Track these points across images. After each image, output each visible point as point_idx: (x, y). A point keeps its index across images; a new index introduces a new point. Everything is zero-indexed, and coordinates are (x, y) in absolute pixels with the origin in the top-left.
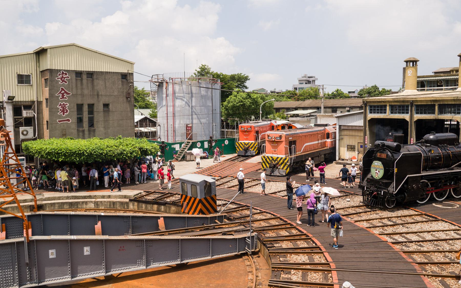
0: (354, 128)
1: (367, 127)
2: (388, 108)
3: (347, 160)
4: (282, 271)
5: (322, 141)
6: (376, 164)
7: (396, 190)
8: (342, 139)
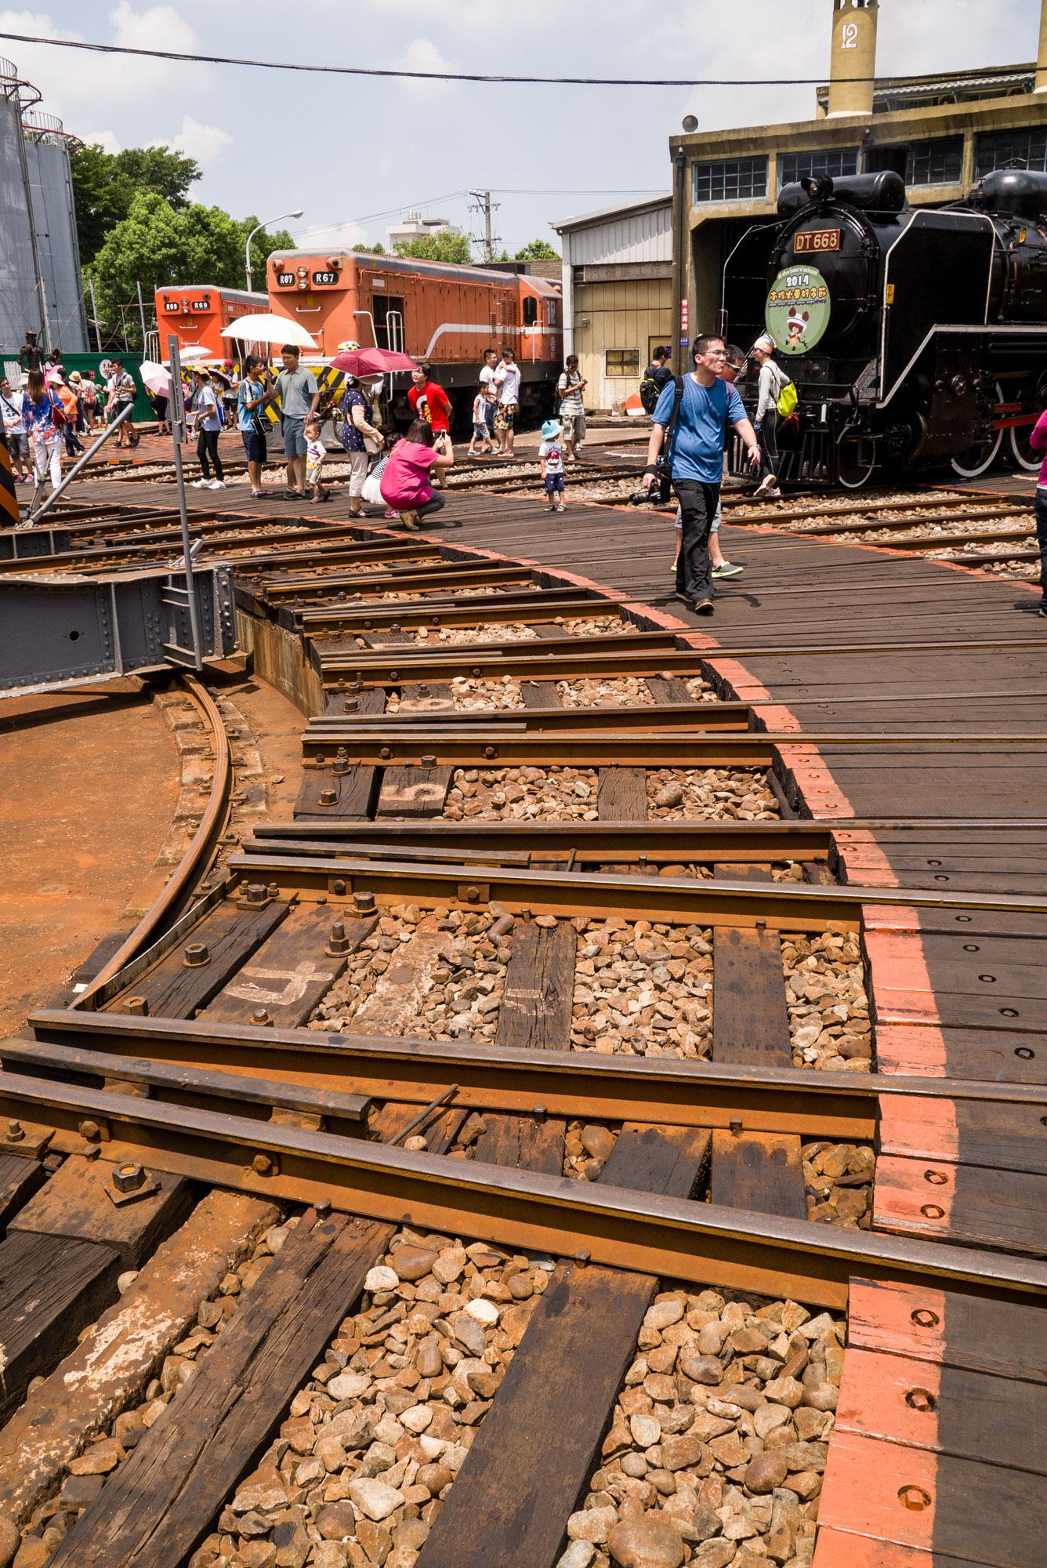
0: (634, 274)
1: (689, 259)
2: (772, 167)
3: (609, 413)
4: (389, 691)
5: (508, 330)
6: (792, 282)
7: (885, 394)
8: (587, 325)
